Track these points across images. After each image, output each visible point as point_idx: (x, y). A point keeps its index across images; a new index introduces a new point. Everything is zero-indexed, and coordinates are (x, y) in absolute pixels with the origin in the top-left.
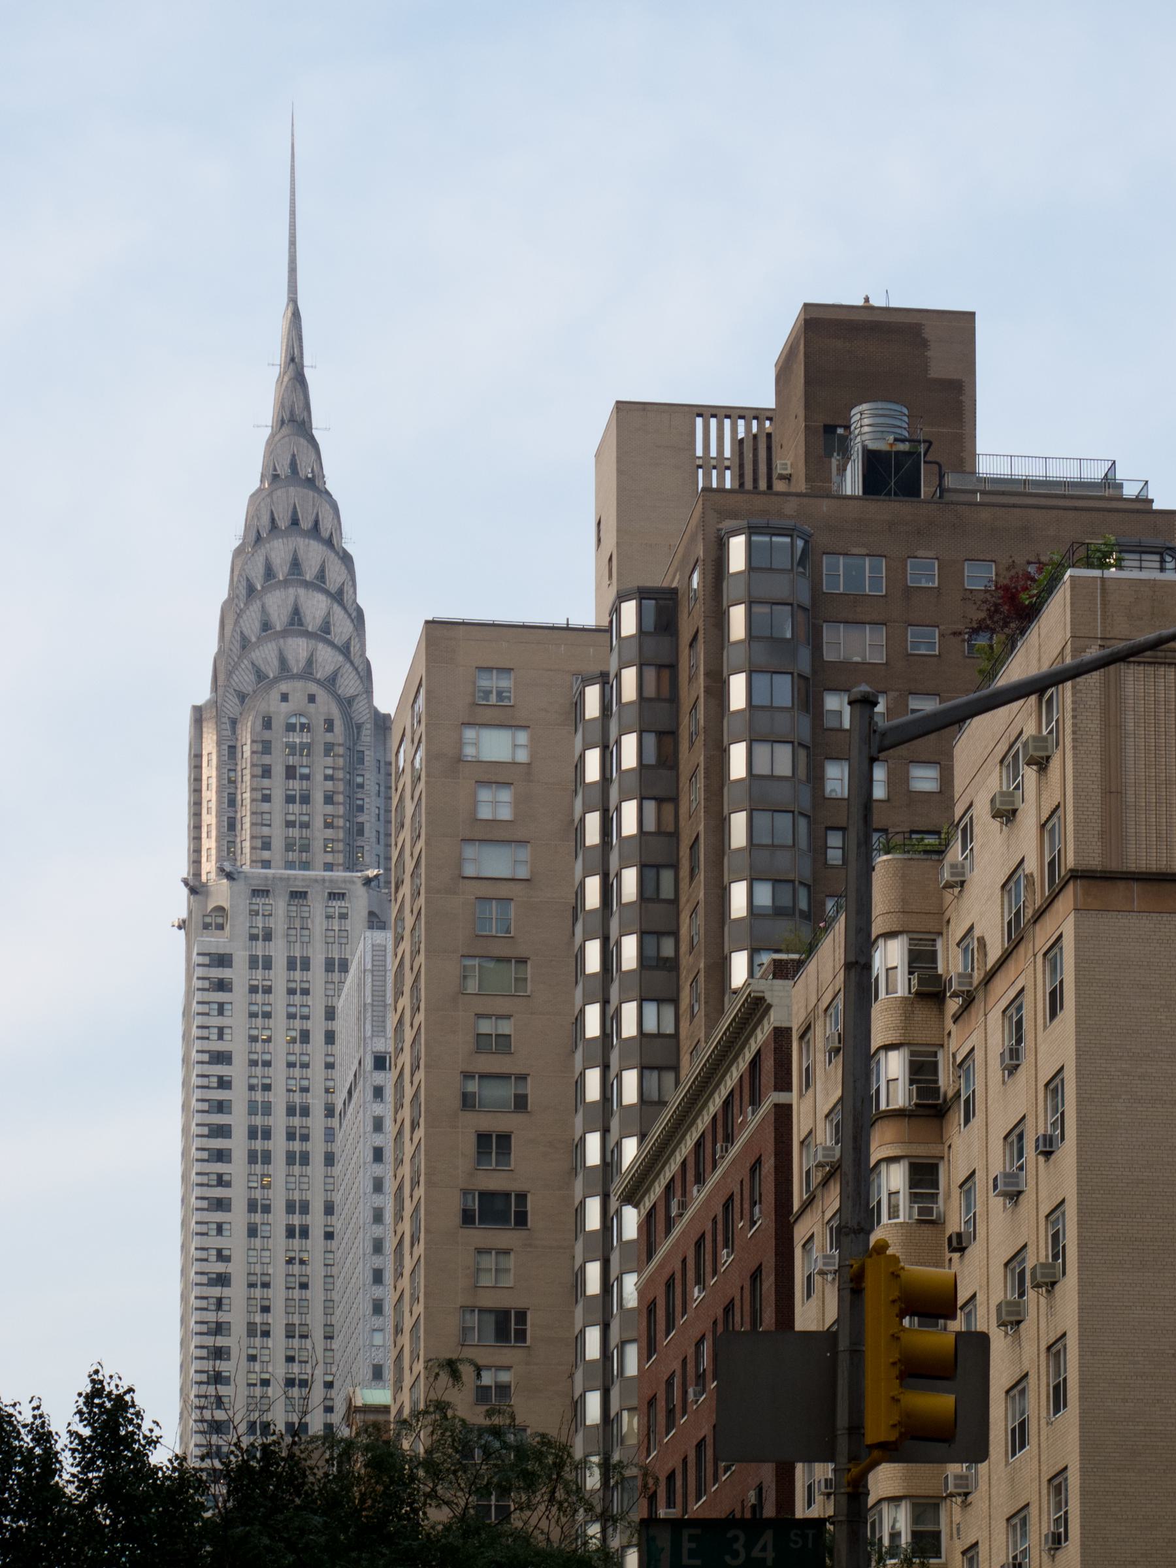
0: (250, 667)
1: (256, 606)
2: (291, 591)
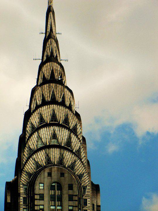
0: (33, 161)
1: (35, 135)
2: (52, 128)
